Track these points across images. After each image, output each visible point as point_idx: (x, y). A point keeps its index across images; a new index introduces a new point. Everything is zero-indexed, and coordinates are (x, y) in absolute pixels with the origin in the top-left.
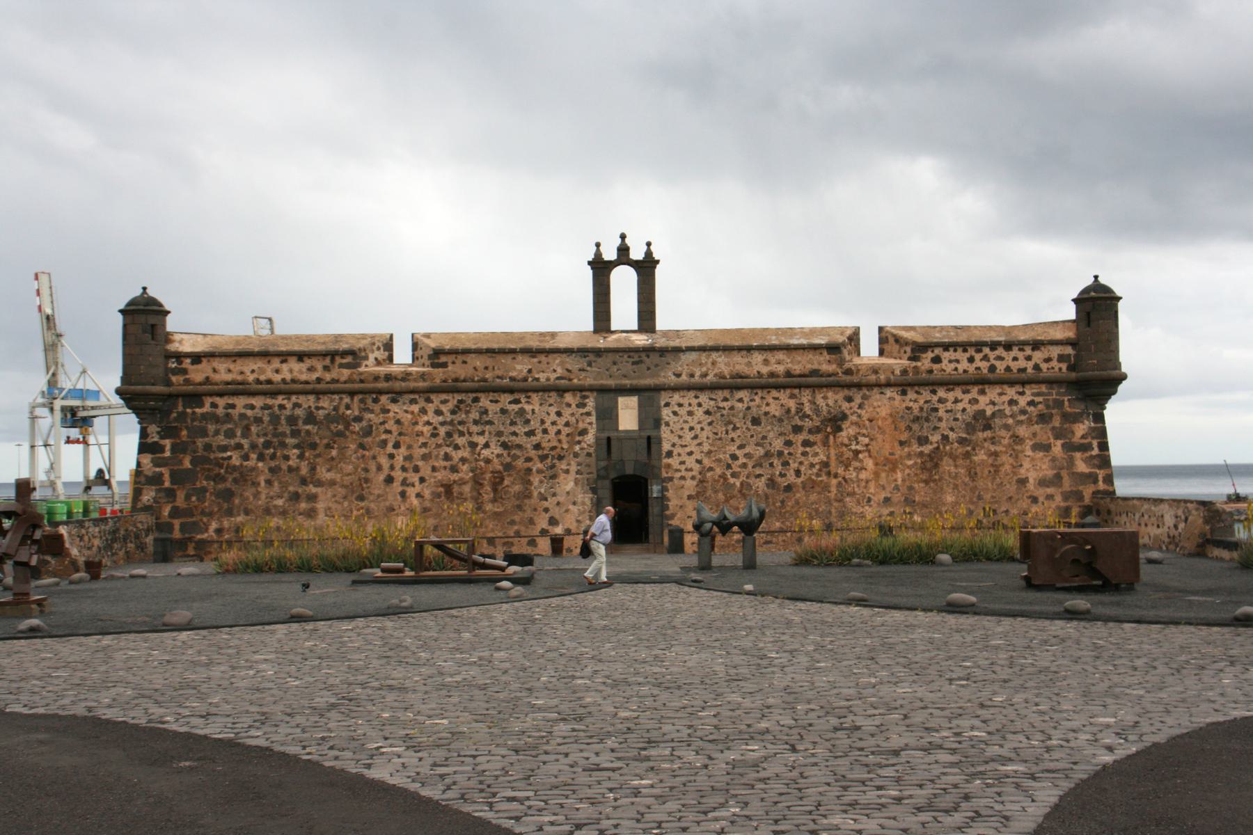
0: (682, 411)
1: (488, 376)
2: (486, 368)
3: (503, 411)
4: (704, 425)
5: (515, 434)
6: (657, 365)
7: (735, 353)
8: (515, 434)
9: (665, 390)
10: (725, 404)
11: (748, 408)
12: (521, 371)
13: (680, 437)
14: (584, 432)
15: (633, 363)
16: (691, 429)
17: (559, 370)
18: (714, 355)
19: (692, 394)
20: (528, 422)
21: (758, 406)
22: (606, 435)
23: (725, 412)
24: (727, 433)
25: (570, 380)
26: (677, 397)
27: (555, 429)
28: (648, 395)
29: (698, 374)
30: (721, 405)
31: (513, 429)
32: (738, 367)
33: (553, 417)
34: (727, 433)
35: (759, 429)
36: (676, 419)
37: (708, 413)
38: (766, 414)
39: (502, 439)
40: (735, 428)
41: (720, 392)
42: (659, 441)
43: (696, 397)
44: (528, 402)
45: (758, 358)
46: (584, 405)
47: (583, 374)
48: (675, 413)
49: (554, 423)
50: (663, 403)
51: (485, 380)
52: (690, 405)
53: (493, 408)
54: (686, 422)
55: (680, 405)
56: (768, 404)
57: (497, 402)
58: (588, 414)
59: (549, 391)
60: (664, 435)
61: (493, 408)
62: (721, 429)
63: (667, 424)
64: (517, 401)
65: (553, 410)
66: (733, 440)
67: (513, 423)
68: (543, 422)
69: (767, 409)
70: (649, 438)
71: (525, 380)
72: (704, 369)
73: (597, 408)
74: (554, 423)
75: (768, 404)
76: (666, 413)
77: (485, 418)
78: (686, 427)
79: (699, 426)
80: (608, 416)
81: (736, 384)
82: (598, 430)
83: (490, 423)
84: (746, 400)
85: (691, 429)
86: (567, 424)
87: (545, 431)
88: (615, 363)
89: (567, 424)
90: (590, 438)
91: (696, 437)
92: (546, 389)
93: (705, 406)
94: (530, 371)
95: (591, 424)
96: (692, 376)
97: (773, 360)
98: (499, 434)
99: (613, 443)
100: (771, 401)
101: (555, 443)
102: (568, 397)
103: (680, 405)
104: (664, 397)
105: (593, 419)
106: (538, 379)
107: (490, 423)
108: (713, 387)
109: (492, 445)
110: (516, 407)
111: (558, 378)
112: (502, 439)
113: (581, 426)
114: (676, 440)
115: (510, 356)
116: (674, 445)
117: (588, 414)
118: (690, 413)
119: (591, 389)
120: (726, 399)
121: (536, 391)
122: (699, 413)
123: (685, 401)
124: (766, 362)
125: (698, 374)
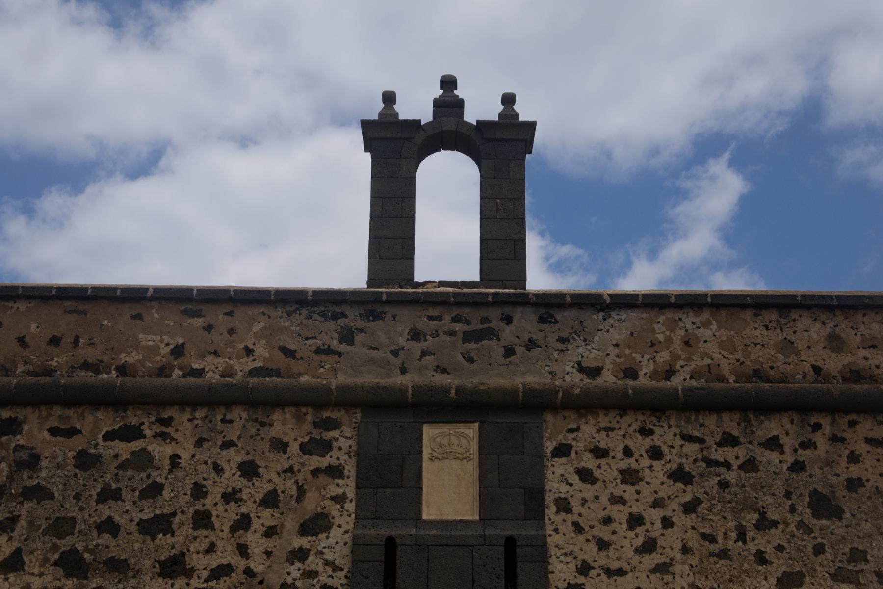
0: (608, 470)
1: (59, 360)
2: (55, 341)
3: (86, 461)
4: (673, 508)
5: (110, 527)
6: (531, 345)
7: (748, 314)
8: (110, 527)
9: (554, 408)
10: (728, 453)
11: (798, 467)
12: (155, 349)
13: (603, 545)
14: (316, 525)
15: (468, 337)
16: (635, 521)
17: (261, 350)
18: (689, 320)
19: (631, 422)
20: (154, 490)
21: (829, 463)
22: (384, 531)
23: (731, 476)
24: (742, 536)
25: (290, 375)
26: (589, 431)
27: (233, 512)
28: (508, 420)
29: (647, 368)
30: (718, 455)
31: (106, 511)
32: (756, 353)
33: (231, 478)
34: (742, 536)
35: (836, 527)
36: (589, 491)
37: (680, 476)
38: (853, 484)
39: (65, 544)
40: (764, 524)
41: (711, 421)
42: (543, 560)
43: (645, 432)
44: (164, 436)
45: (811, 331)
46: (325, 447)
47: (329, 362)
48: (586, 476)
49: (231, 497)
50: (550, 446)
51: (49, 372)
52: (628, 452)
53: (57, 453)
54: (621, 501)
55: (600, 453)
56: (854, 458)
57: (72, 432)
58: (335, 472)
59: (229, 404)
60: (553, 540)
61: (57, 453)
62: (723, 526)
63: (563, 506)
64: (130, 433)
65: (233, 458)
66: (761, 558)
67: (108, 495)
68: (199, 492)
69: (854, 471)
70: (510, 544)
71: (163, 371)
72: (663, 357)
73: (361, 456)
74: (231, 497)
75: (854, 458)
76: (558, 478)
77: (26, 479)
78: (620, 513)
79: (655, 515)
80: (390, 479)
81: (754, 401)
82: (359, 518)
83: (39, 494)
84: (788, 442)
85: (635, 521)
86: (270, 500)
87: (203, 520)
88: (416, 335)
89: (270, 500)
90: (336, 543)
91: (649, 546)
92: (217, 399)
93: (672, 460)
94: (178, 351)
95: (340, 499)
96: (631, 373)
97: (854, 339)
98: (61, 526)
99: (403, 557)
100: (862, 448)
101: (226, 555)
102: (283, 425)
103: (600, 453)
104: (553, 430)
105: (348, 486)
106: (200, 373)
107: (39, 494)
108: (693, 405)
109: (31, 563)
110: (125, 449)
111: (254, 372)
112: (65, 544)
113: (311, 503)
114: (590, 552)
115: (128, 311)
116: (584, 569)
117: (335, 472)
118: (630, 477)
119: (348, 400)
120: (729, 441)
121: (189, 401)
122: (656, 476)
123: (614, 443)
124: (835, 343)
125: (647, 368)
